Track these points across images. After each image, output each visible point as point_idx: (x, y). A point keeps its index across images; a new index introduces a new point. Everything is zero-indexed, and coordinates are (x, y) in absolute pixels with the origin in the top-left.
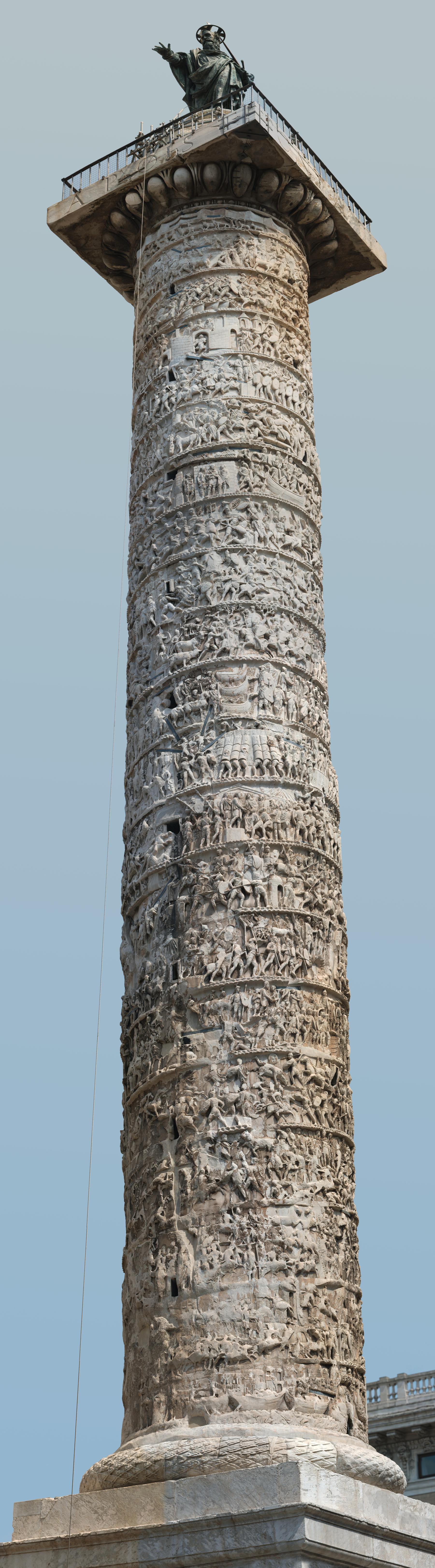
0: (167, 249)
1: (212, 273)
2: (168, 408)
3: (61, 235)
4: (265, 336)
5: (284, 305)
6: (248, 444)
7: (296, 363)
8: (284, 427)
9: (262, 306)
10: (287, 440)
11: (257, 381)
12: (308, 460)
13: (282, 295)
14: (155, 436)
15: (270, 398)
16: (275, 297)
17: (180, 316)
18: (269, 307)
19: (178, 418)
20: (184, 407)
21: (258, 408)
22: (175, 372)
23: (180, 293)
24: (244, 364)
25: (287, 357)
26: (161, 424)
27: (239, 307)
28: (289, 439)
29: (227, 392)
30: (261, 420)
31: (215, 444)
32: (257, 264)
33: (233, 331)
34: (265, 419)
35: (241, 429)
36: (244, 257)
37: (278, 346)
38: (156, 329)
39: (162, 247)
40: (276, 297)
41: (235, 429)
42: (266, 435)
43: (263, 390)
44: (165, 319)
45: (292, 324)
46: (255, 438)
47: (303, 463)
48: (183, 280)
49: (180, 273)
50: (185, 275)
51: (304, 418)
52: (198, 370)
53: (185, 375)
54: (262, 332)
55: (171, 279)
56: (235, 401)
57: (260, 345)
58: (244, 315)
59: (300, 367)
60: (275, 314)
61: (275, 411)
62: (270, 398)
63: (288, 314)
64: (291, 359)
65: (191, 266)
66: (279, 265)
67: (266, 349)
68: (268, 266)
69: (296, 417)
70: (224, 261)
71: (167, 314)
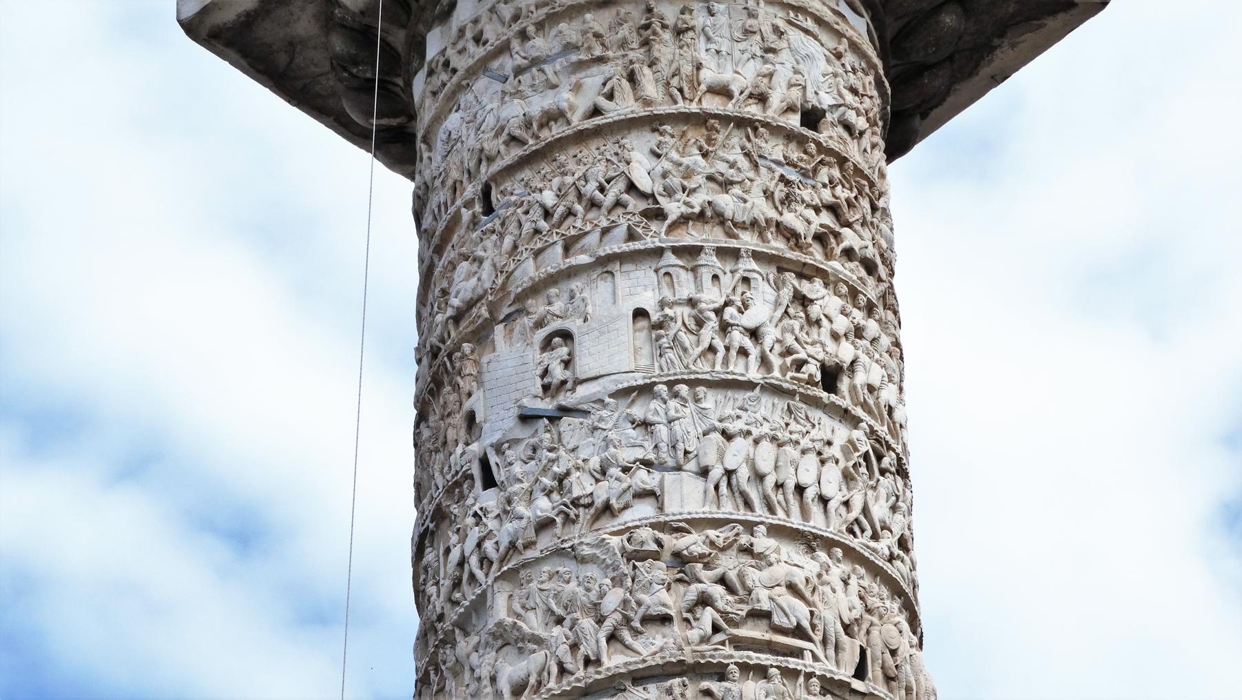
0: (472, 72)
1: (582, 137)
2: (480, 574)
3: (220, 47)
4: (730, 312)
5: (788, 200)
6: (681, 662)
7: (831, 376)
8: (792, 588)
9: (720, 218)
10: (799, 626)
11: (710, 459)
12: (873, 670)
13: (780, 171)
14: (451, 661)
15: (748, 505)
16: (758, 181)
17: (504, 284)
18: (739, 219)
19: (500, 609)
20: (515, 571)
21: (712, 544)
22: (493, 459)
23: (502, 212)
24: (672, 413)
25: (799, 365)
26: (463, 626)
27: (655, 236)
28: (806, 624)
29: (626, 507)
30: (722, 580)
31: (593, 675)
32: (703, 87)
33: (640, 314)
34: (732, 576)
35: (665, 619)
36: (667, 72)
37: (771, 335)
38: (451, 327)
39: (461, 63)
40: (765, 179)
41: (647, 620)
42: (736, 624)
43: (729, 484)
44: (468, 295)
45: (816, 256)
46: (704, 640)
47: (857, 685)
48: (510, 170)
49: (502, 148)
50: (517, 152)
51: (858, 543)
52: (551, 450)
53: (518, 469)
54: (722, 301)
55: (483, 169)
56: (646, 534)
57: (719, 344)
58: (670, 258)
59: (844, 384)
60: (761, 235)
61: (763, 542)
62: (748, 505)
63: (800, 227)
64: (813, 369)
65: (528, 124)
66: (770, 75)
67: (733, 353)
68: (735, 89)
69: (829, 544)
70: (610, 96)
71: (474, 281)
